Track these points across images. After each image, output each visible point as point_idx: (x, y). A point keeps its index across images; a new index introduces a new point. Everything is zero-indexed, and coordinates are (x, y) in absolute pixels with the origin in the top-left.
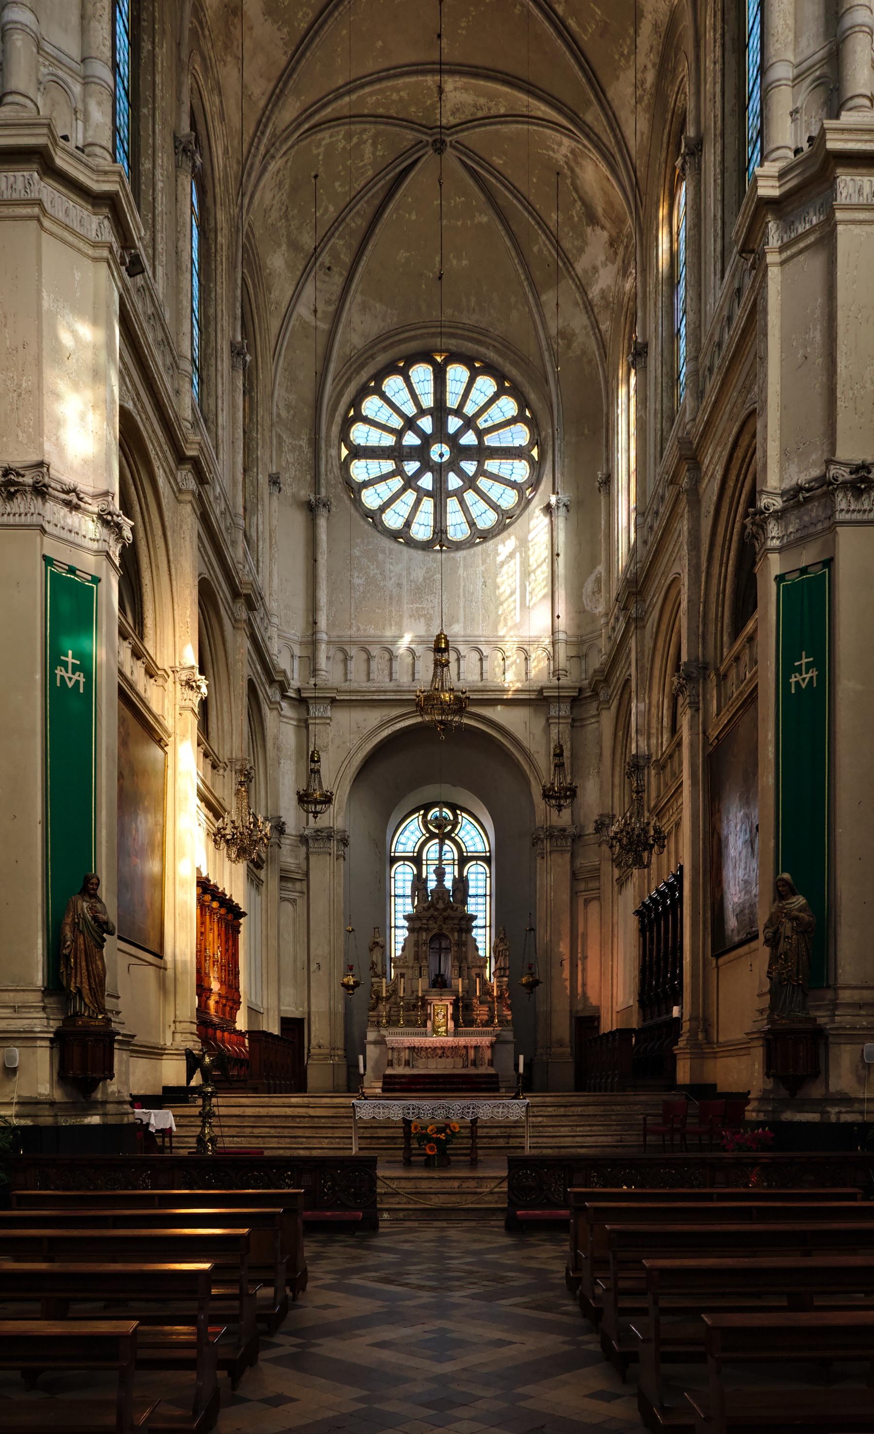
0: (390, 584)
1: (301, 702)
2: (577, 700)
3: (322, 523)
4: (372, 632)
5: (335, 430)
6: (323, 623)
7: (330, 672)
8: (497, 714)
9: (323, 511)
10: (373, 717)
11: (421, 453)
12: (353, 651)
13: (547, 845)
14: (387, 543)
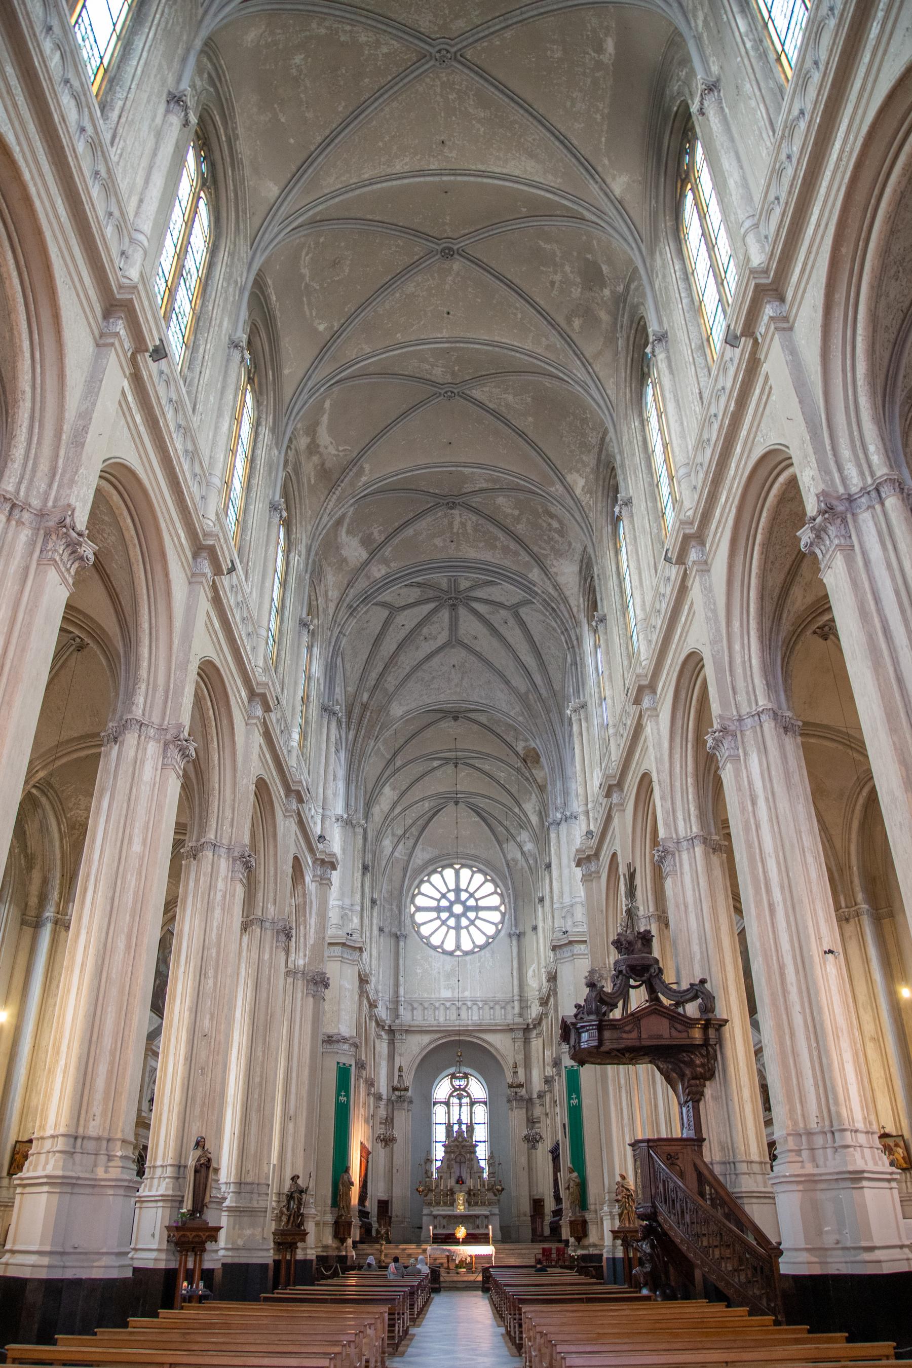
0: (435, 972)
1: (391, 1031)
2: (527, 1030)
3: (402, 944)
4: (425, 995)
5: (409, 900)
6: (401, 991)
7: (405, 1016)
8: (489, 1037)
9: (402, 939)
10: (426, 1039)
11: (449, 909)
12: (415, 1005)
13: (514, 1103)
14: (432, 952)
